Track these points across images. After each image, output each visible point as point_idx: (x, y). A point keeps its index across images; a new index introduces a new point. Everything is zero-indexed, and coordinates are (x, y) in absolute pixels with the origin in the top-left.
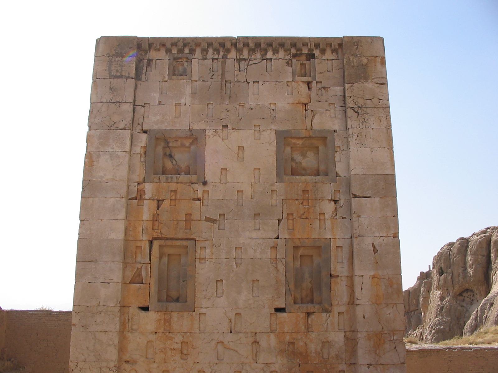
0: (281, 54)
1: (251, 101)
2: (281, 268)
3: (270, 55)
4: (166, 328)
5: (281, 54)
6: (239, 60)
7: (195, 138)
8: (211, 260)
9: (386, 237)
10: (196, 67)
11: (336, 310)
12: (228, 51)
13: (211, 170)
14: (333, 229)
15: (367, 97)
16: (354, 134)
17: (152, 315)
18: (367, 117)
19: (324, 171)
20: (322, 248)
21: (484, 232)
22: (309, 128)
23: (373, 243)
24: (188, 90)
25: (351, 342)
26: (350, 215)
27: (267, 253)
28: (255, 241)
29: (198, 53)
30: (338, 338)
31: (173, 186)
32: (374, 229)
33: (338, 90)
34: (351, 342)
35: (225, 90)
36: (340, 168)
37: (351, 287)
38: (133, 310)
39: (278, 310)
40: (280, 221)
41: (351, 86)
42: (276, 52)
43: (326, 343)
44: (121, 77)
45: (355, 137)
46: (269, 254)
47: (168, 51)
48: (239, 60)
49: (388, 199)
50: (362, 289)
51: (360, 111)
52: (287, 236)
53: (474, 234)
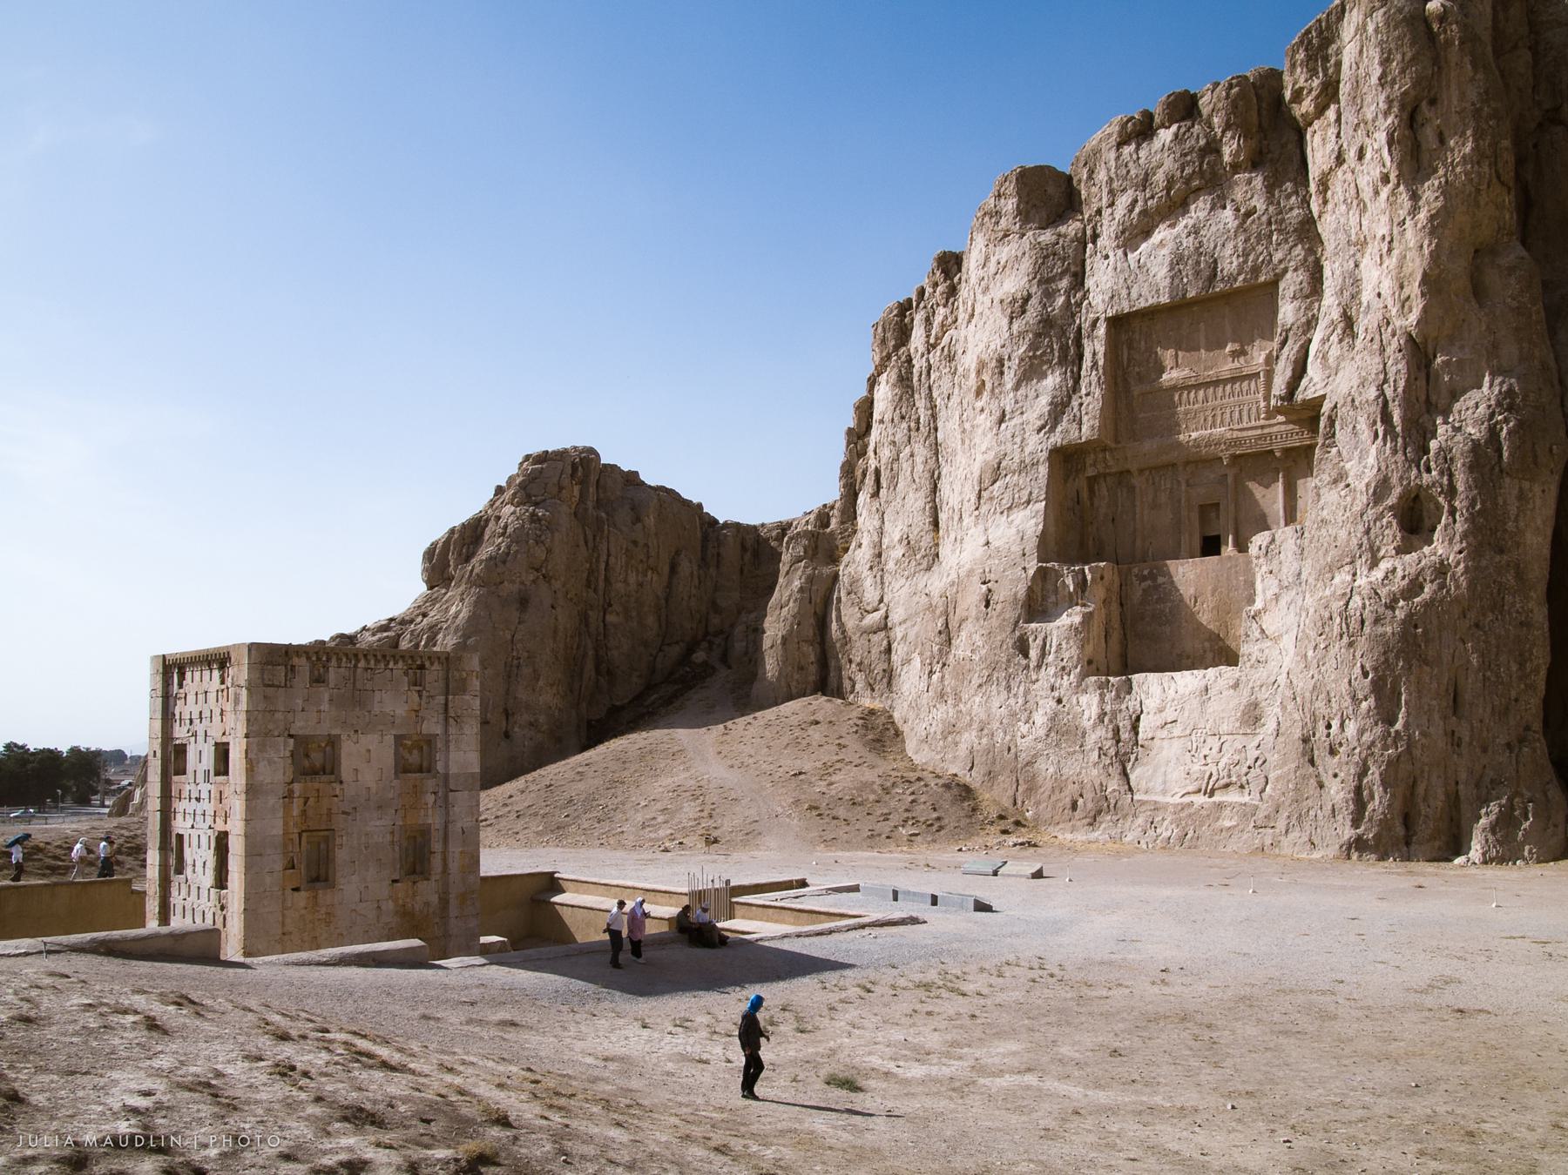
0: (400, 664)
1: (376, 709)
3: (391, 665)
4: (315, 902)
5: (400, 664)
6: (366, 669)
7: (333, 742)
10: (332, 675)
11: (433, 878)
12: (358, 661)
13: (346, 771)
17: (303, 895)
19: (426, 768)
20: (425, 832)
21: (384, 628)
24: (326, 697)
25: (444, 902)
26: (446, 805)
28: (378, 828)
29: (334, 662)
30: (434, 899)
31: (316, 785)
33: (441, 699)
34: (444, 902)
35: (355, 698)
36: (440, 767)
37: (445, 860)
38: (288, 892)
39: (395, 881)
42: (396, 663)
43: (427, 904)
44: (272, 686)
46: (389, 837)
47: (308, 658)
48: (366, 669)
53: (364, 628)
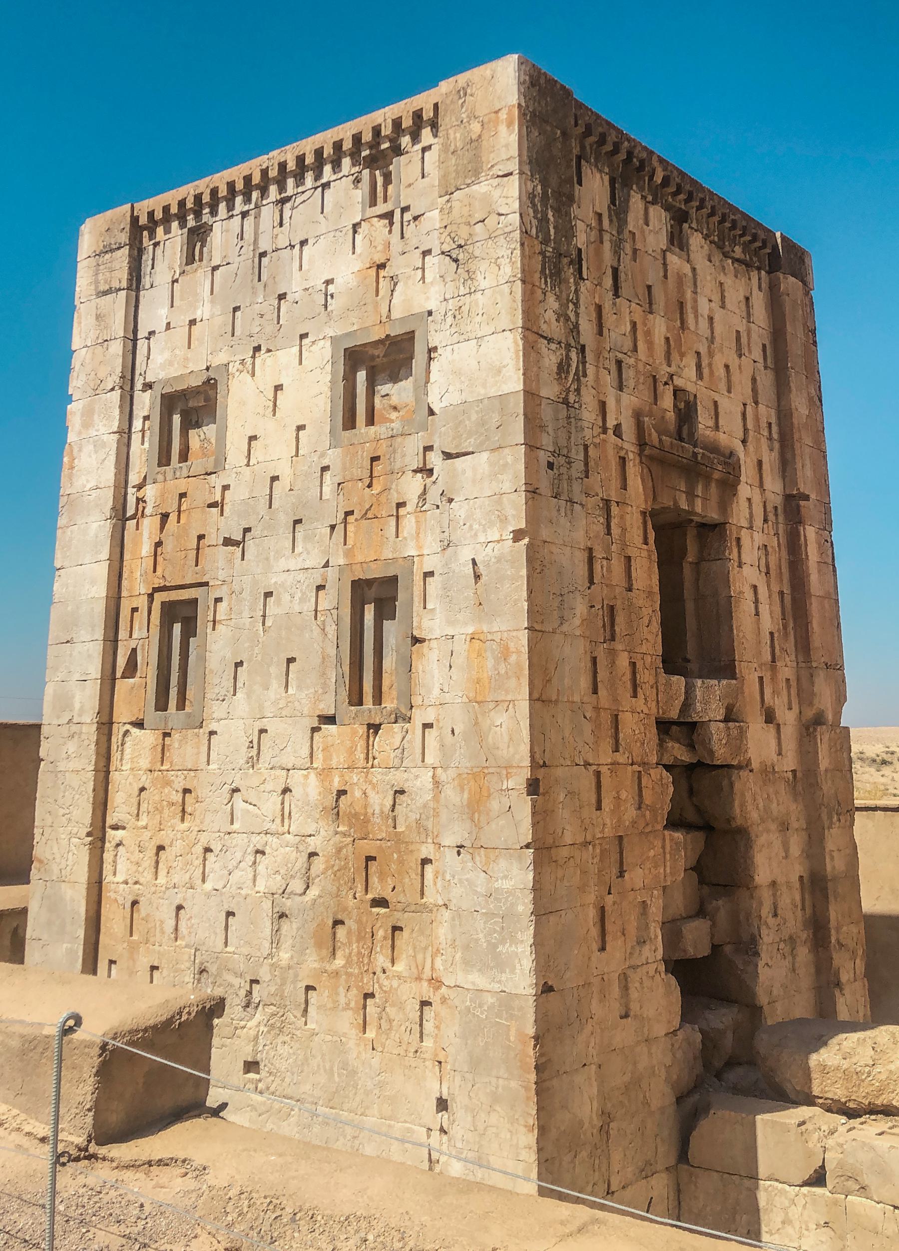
2: (331, 629)
8: (228, 622)
9: (498, 541)
14: (418, 534)
15: (478, 216)
16: (449, 314)
18: (472, 266)
22: (384, 319)
23: (474, 561)
27: (309, 601)
32: (476, 526)
40: (333, 527)
41: (448, 201)
45: (450, 320)
49: (507, 451)
50: (451, 667)
51: (460, 257)
52: (342, 561)
